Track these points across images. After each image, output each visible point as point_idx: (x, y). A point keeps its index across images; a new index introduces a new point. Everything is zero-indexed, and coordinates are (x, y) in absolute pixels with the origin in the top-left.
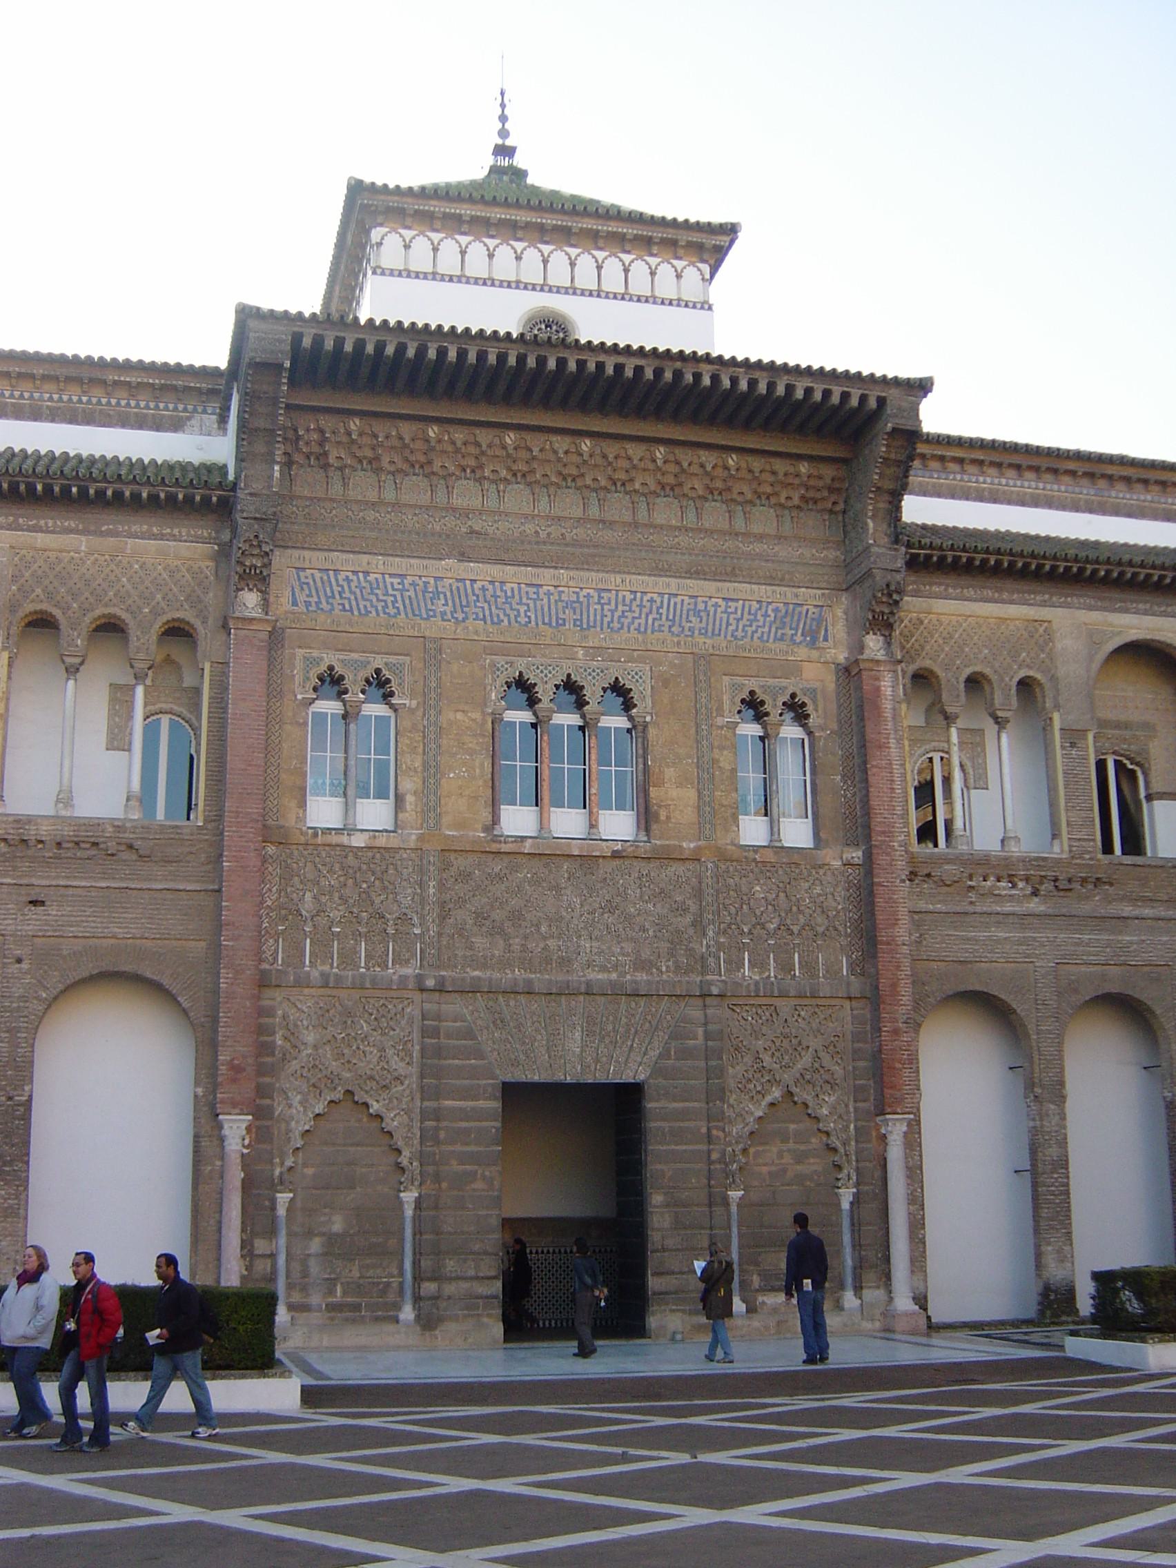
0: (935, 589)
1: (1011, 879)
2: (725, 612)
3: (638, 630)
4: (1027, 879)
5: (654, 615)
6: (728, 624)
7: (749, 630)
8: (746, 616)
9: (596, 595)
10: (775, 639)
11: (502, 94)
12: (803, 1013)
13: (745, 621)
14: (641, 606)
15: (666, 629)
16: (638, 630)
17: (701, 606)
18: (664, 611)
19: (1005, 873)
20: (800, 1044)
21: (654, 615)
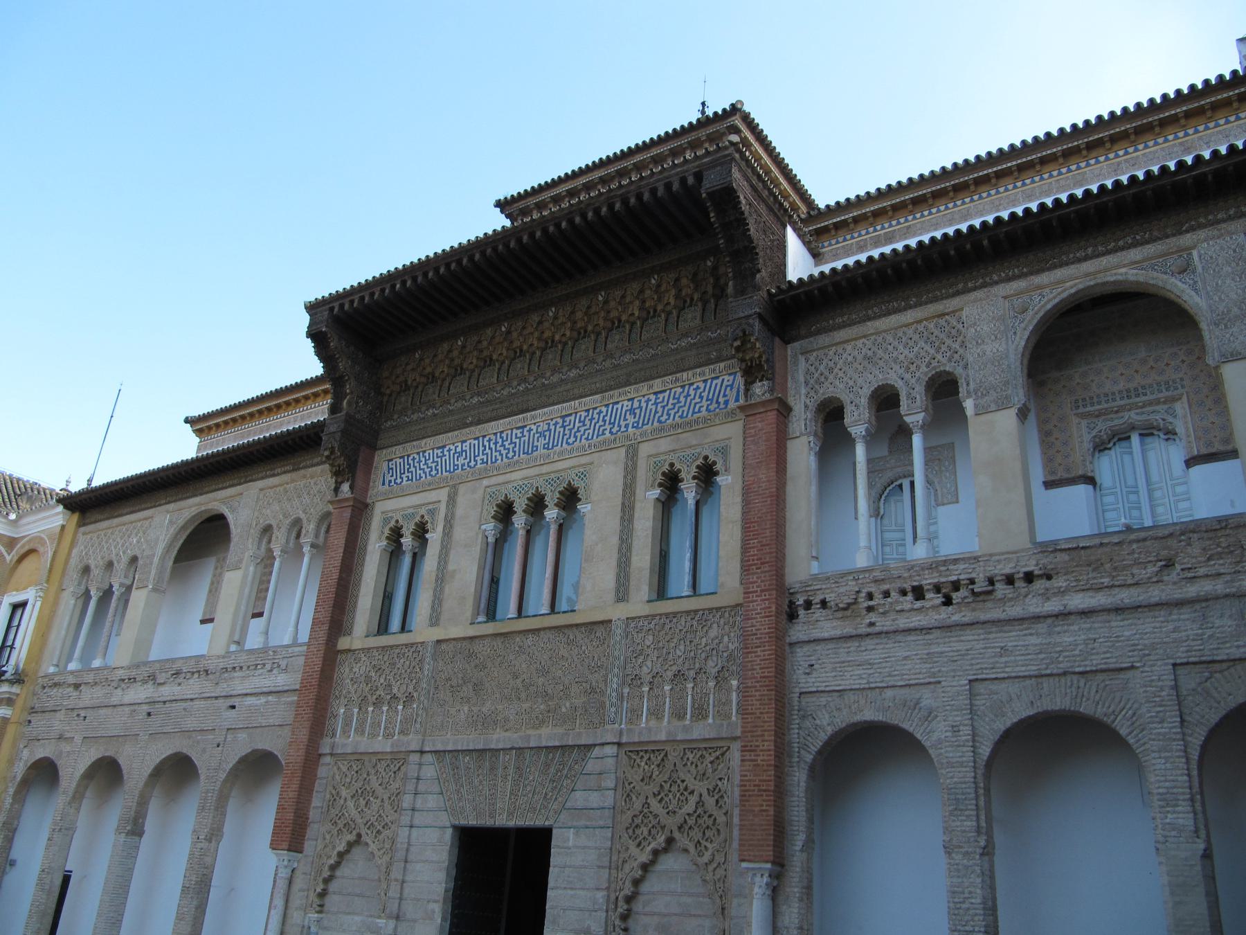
0: (839, 320)
1: (919, 593)
2: (656, 404)
3: (587, 439)
4: (937, 588)
5: (601, 423)
6: (656, 412)
7: (672, 413)
8: (671, 401)
9: (560, 421)
10: (694, 413)
11: (703, 104)
12: (691, 756)
13: (670, 406)
14: (591, 420)
15: (607, 432)
16: (587, 439)
17: (636, 404)
18: (607, 418)
19: (907, 586)
20: (686, 789)
21: (601, 423)
